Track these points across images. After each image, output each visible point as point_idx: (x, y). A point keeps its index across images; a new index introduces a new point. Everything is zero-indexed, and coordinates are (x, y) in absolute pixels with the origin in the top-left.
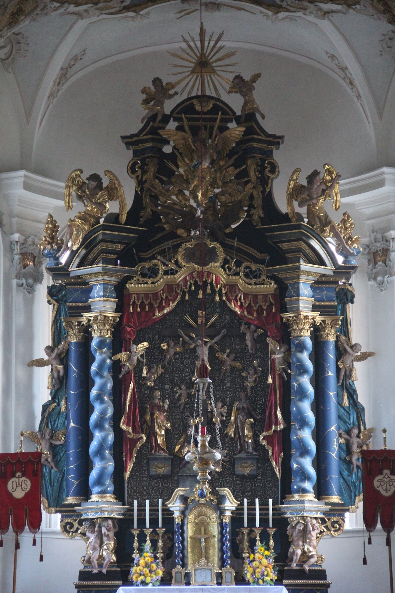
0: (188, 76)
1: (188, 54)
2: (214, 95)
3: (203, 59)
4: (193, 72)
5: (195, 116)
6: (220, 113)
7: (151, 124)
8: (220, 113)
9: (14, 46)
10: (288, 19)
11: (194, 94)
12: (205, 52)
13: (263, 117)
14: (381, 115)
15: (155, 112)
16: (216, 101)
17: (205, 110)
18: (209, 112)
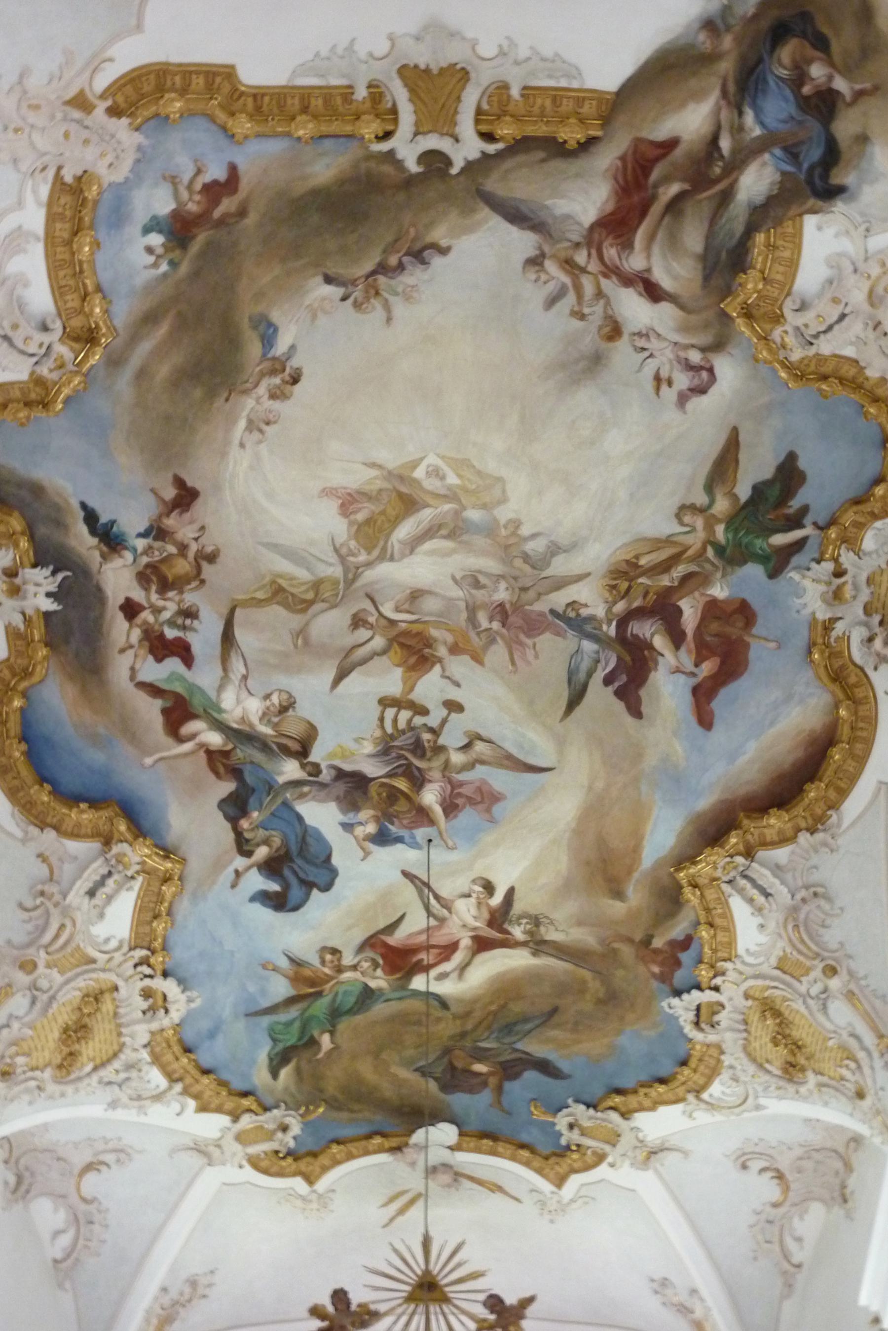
0: (400, 1305)
9: (82, 1230)
10: (580, 1201)
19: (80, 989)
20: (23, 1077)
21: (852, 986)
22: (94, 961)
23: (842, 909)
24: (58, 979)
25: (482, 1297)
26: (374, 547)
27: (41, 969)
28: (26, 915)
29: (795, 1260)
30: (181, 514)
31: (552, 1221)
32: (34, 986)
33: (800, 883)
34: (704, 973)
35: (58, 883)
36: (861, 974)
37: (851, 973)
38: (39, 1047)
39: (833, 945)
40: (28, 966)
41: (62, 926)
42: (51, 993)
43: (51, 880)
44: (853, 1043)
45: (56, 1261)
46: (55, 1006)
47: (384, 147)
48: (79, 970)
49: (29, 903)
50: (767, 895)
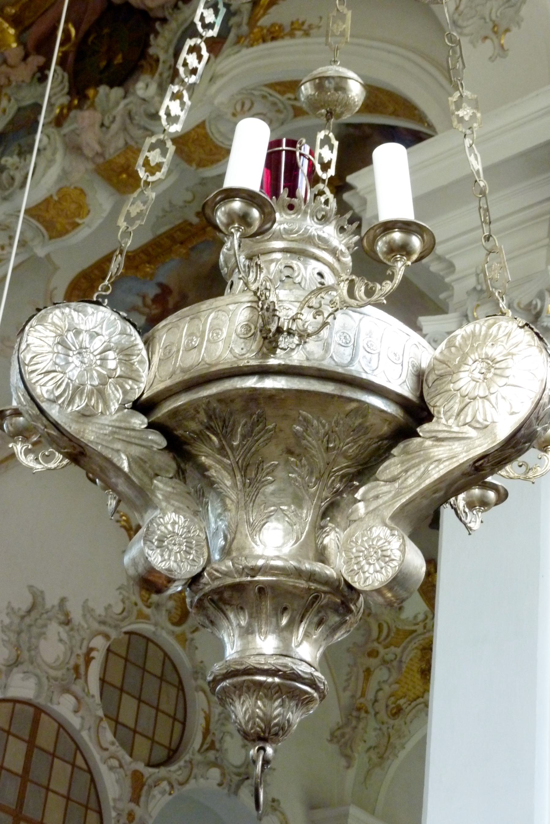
19: (416, 648)
20: (410, 708)
22: (415, 631)
24: (398, 650)
27: (382, 651)
32: (385, 662)
38: (410, 687)
40: (373, 654)
42: (398, 659)
46: (404, 666)
48: (408, 639)
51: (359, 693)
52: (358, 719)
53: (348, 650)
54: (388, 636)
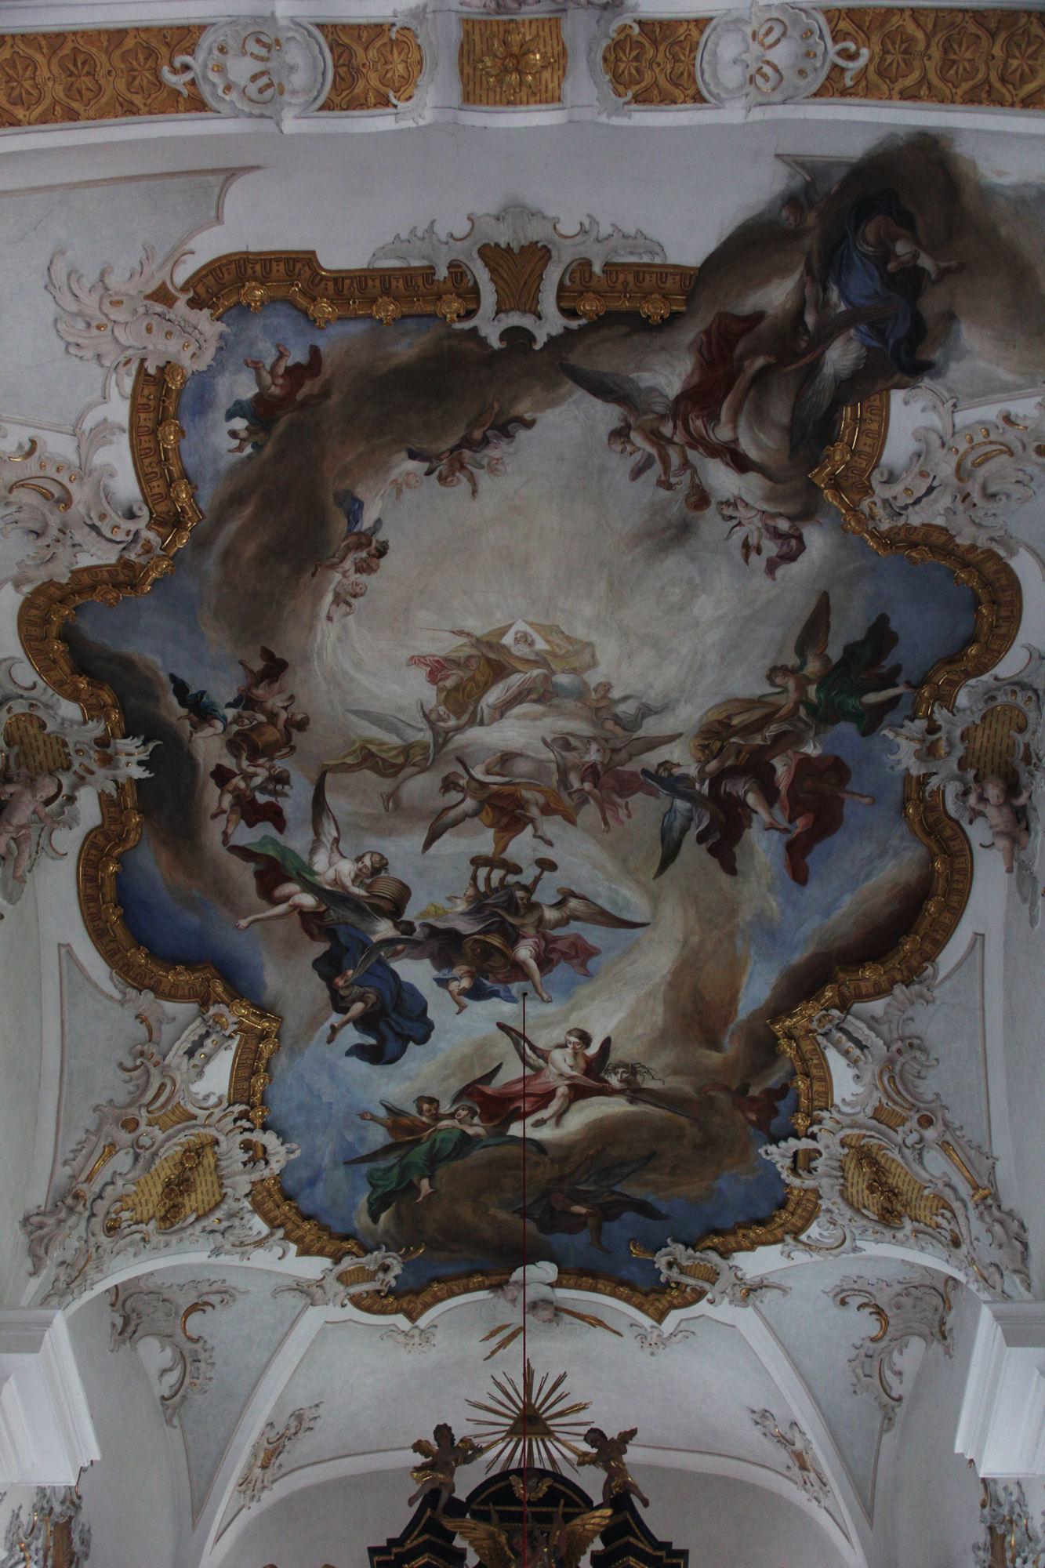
1: (503, 1405)
2: (548, 1467)
3: (529, 1412)
4: (511, 1432)
5: (513, 1509)
6: (562, 1501)
7: (429, 1513)
8: (562, 1501)
9: (188, 1366)
10: (680, 1336)
11: (514, 1465)
12: (533, 1401)
13: (646, 1503)
14: (869, 1514)
15: (436, 1485)
16: (555, 1481)
17: (532, 1496)
18: (540, 1502)
19: (181, 1144)
20: (127, 1231)
21: (948, 1137)
22: (195, 1117)
23: (937, 1060)
24: (160, 1136)
25: (584, 1430)
26: (464, 712)
27: (143, 1127)
28: (126, 1075)
29: (894, 1394)
30: (270, 684)
31: (652, 1354)
32: (136, 1144)
33: (895, 1035)
34: (801, 1122)
35: (158, 1044)
36: (957, 1124)
37: (946, 1124)
38: (143, 1200)
39: (929, 1097)
40: (131, 1125)
41: (163, 1086)
42: (153, 1149)
43: (150, 1041)
44: (948, 1194)
45: (163, 1398)
46: (157, 1162)
47: (467, 325)
48: (180, 1126)
49: (129, 1064)
50: (862, 1047)
51: (83, 1177)
52: (71, 1210)
53: (96, 1108)
54: (163, 1106)
